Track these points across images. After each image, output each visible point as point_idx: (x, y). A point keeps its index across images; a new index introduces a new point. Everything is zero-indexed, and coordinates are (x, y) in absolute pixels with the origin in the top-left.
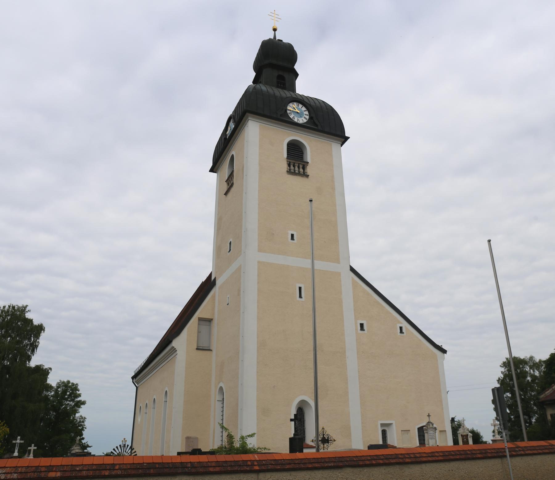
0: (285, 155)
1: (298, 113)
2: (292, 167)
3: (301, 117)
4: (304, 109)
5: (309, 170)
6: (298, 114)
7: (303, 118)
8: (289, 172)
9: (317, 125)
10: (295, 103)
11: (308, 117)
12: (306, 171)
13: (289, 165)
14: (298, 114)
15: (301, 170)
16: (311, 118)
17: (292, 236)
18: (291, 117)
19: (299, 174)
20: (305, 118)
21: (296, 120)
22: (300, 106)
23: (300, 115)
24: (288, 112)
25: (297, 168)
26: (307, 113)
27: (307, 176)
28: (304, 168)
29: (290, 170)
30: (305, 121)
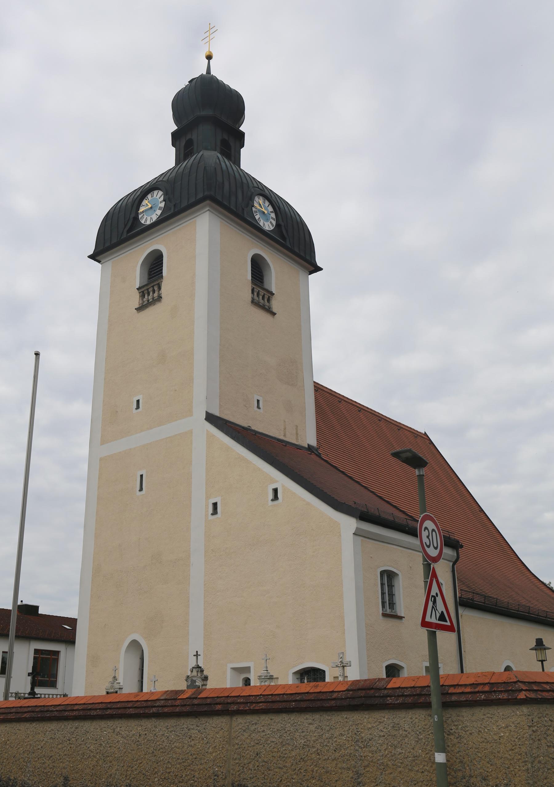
0: (249, 277)
1: (264, 213)
3: (267, 220)
4: (270, 209)
5: (275, 305)
7: (269, 223)
9: (284, 238)
10: (261, 198)
11: (274, 223)
16: (278, 225)
18: (257, 217)
20: (271, 222)
21: (261, 224)
22: (267, 203)
24: (254, 209)
26: (273, 215)
27: (274, 314)
28: (269, 300)
30: (272, 228)
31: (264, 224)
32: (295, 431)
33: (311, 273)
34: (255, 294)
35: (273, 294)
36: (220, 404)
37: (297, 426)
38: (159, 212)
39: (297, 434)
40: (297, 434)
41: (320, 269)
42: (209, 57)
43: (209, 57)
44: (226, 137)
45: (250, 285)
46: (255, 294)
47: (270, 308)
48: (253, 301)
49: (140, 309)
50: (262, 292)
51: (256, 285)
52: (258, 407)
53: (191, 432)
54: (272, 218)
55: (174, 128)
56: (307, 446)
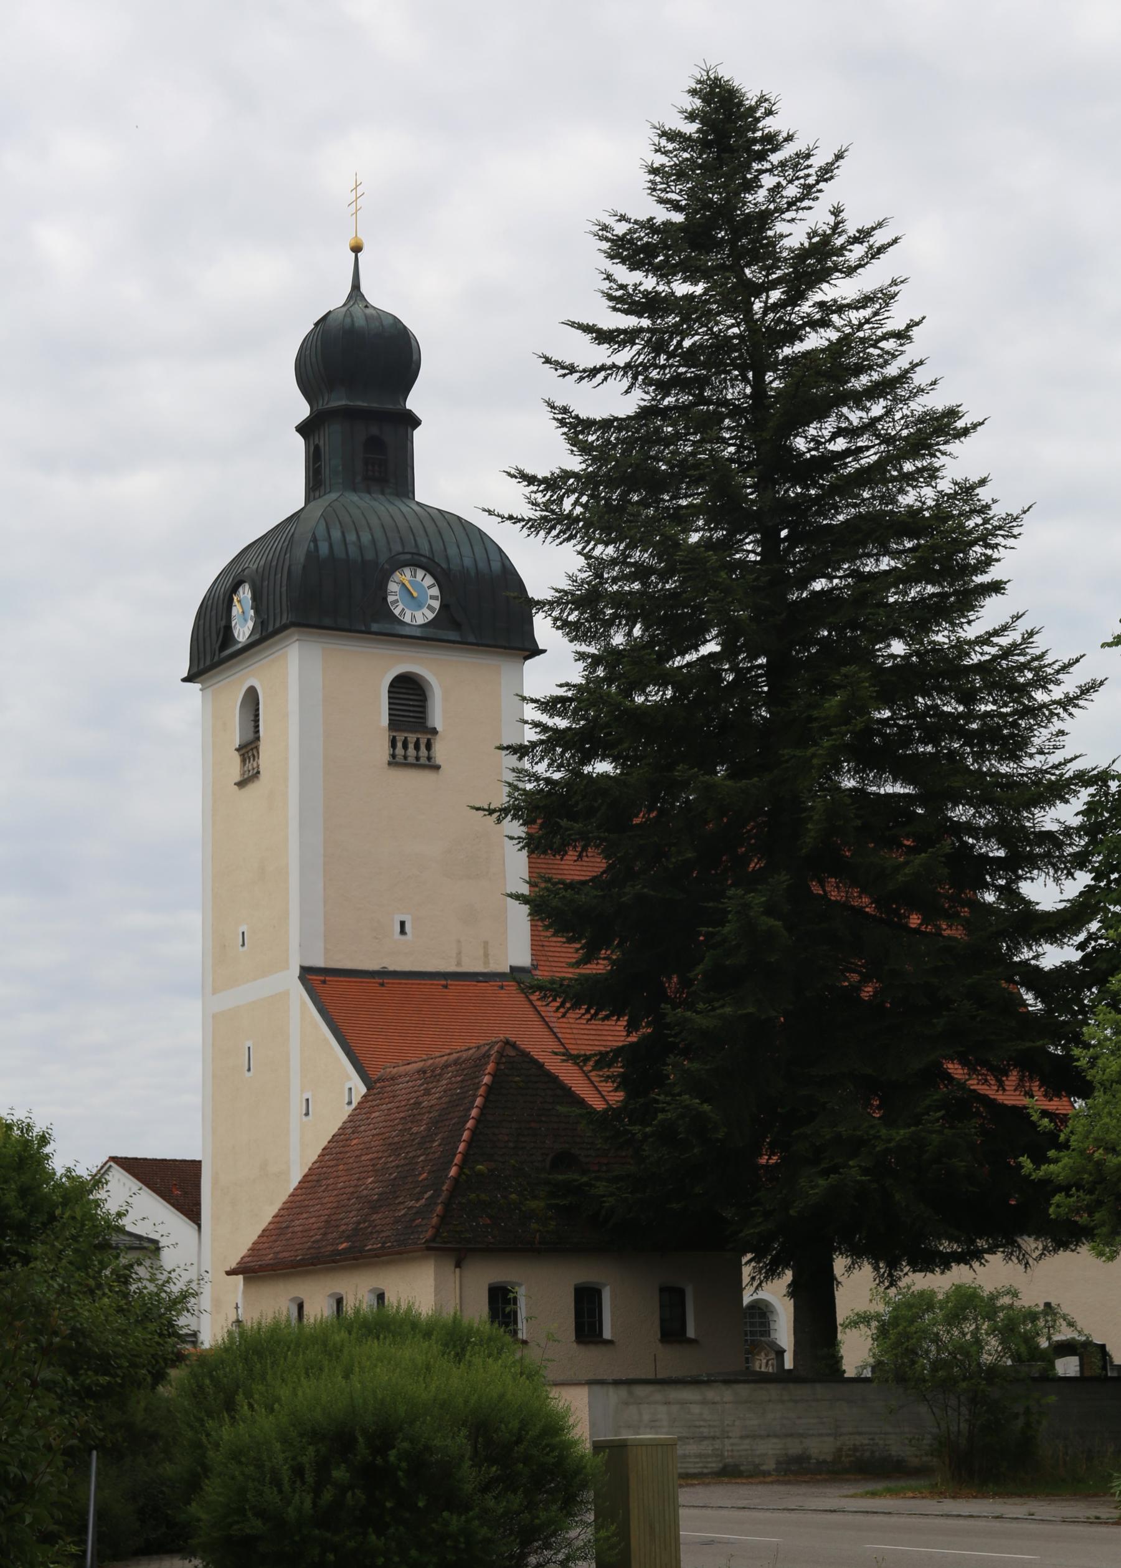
0: (385, 721)
2: (399, 750)
3: (420, 606)
4: (429, 580)
5: (441, 751)
6: (415, 597)
8: (394, 762)
9: (457, 626)
10: (407, 571)
11: (436, 604)
12: (433, 755)
13: (393, 743)
14: (415, 597)
15: (423, 751)
16: (443, 606)
17: (402, 924)
18: (397, 612)
19: (417, 765)
20: (430, 608)
21: (407, 619)
22: (420, 573)
23: (417, 603)
24: (390, 599)
25: (411, 751)
26: (435, 591)
27: (437, 768)
28: (429, 746)
29: (393, 756)
31: (413, 617)
32: (481, 952)
33: (527, 658)
34: (399, 745)
35: (434, 731)
36: (325, 949)
37: (486, 943)
38: (251, 624)
39: (486, 955)
40: (486, 955)
41: (544, 651)
42: (357, 249)
43: (357, 249)
44: (374, 430)
45: (387, 734)
46: (399, 745)
47: (429, 758)
48: (394, 762)
49: (241, 784)
50: (412, 738)
51: (396, 730)
52: (403, 931)
53: (287, 994)
54: (432, 597)
55: (302, 410)
56: (508, 970)
